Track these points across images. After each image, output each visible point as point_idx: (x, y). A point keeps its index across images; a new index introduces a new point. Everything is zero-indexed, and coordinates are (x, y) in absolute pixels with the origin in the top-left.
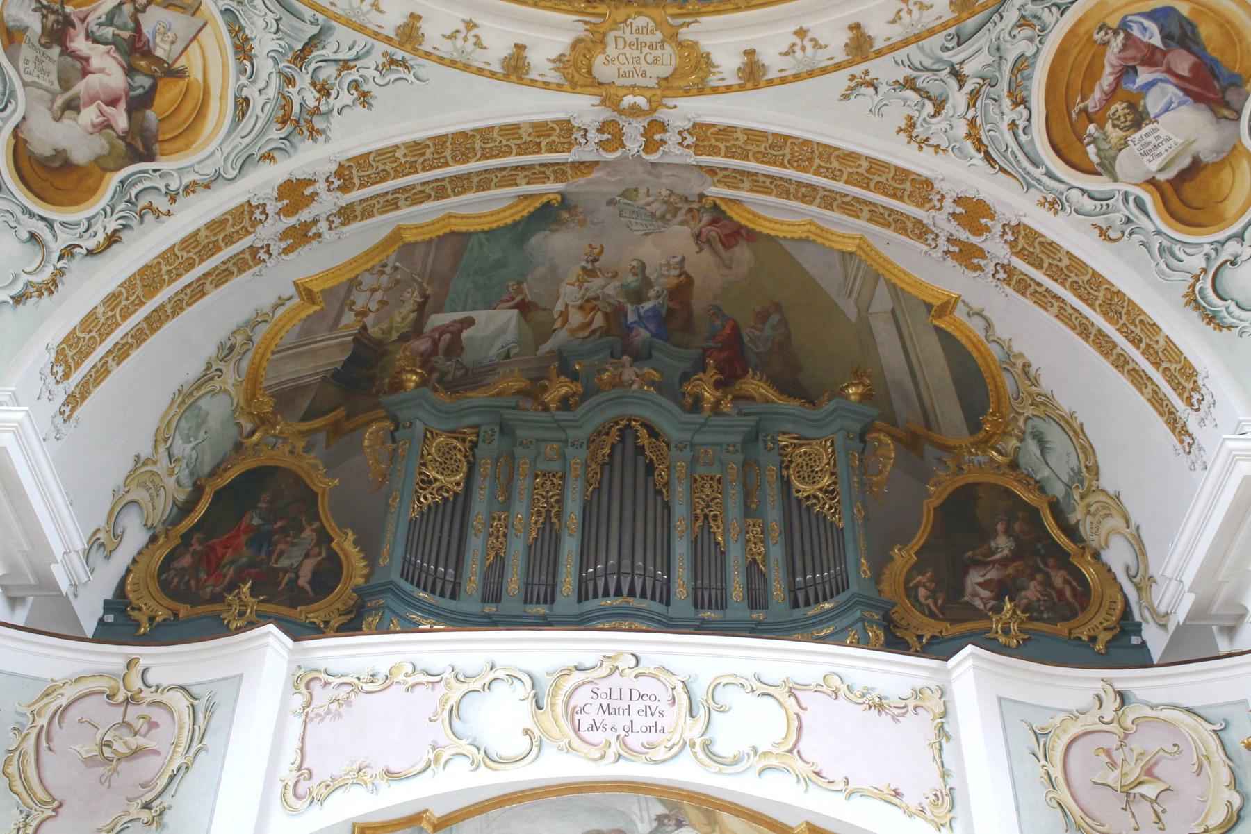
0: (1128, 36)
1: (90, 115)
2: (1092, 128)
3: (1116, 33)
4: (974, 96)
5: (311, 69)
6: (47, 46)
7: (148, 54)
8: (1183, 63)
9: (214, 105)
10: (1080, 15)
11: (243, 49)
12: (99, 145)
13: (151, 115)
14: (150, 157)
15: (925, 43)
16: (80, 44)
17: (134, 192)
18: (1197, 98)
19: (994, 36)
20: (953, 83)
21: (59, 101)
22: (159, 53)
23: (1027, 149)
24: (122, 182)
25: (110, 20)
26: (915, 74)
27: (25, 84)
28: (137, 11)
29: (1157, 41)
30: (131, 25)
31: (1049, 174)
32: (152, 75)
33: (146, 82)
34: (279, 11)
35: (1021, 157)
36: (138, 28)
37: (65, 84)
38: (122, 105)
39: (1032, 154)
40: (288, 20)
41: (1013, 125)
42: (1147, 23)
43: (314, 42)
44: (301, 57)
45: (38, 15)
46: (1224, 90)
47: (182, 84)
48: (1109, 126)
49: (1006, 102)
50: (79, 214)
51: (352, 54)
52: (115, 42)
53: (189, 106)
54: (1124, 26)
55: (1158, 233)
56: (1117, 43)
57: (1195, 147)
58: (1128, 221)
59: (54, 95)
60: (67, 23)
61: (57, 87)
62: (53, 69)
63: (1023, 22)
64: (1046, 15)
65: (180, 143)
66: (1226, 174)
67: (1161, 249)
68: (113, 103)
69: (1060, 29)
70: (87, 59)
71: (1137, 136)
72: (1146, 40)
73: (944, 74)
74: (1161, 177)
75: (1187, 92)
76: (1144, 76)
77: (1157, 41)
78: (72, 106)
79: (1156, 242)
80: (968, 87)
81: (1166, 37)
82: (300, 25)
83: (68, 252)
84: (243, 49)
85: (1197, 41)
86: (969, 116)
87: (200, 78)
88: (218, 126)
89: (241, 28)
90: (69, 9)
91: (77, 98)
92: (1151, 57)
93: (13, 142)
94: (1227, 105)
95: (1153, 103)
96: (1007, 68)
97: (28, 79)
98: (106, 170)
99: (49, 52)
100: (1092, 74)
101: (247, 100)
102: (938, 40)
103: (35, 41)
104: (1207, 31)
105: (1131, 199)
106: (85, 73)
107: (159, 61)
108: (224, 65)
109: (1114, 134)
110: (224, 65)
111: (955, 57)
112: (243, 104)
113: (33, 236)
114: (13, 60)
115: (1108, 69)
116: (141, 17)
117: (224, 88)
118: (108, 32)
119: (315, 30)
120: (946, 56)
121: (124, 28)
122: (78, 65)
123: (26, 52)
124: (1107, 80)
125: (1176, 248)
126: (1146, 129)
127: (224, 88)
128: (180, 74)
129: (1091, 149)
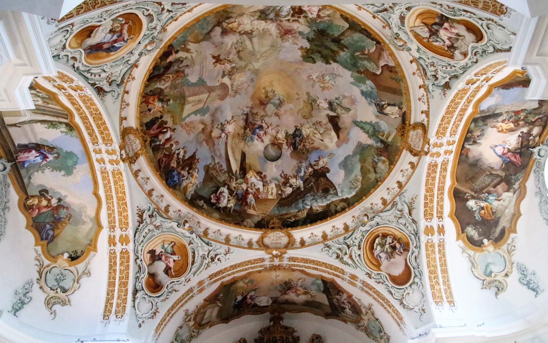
0: (123, 40)
1: (455, 31)
2: (124, 22)
3: (128, 39)
4: (163, 9)
5: (383, 7)
6: (457, 47)
7: (430, 31)
8: (105, 46)
9: (417, 13)
10: (139, 38)
11: (402, 19)
12: (455, 25)
13: (437, 20)
14: (442, 15)
15: (181, 13)
16: (448, 43)
17: (452, 13)
18: (98, 44)
19: (162, 23)
20: (170, 9)
21: (461, 38)
22: (427, 29)
23: (141, 9)
24: (454, 16)
25: (437, 41)
26: (184, 6)
27: (468, 46)
28: (429, 39)
29: (116, 45)
30: (432, 37)
31: (132, 9)
32: (431, 27)
33: (434, 26)
34: (388, 20)
35: (142, 7)
36: (430, 36)
37: (457, 40)
38: (443, 27)
39: (139, 9)
40: (387, 18)
41: (148, 10)
42: (121, 45)
43: (380, 12)
44: (386, 10)
45: (455, 53)
46: (92, 50)
47: (424, 21)
48: (119, 25)
49: (152, 13)
50: (471, 20)
51: (368, 6)
52: (438, 37)
53: (424, 17)
54: (126, 42)
55: (91, 22)
56: (126, 37)
57: (91, 38)
58: (101, 17)
59: (462, 40)
60: (448, 47)
61: (460, 41)
62: (458, 43)
63: (155, 28)
64: (149, 32)
65: (431, 12)
66: (79, 41)
67: (88, 21)
68: (446, 29)
69: (144, 31)
70: (448, 39)
71: (109, 29)
72: (119, 43)
73: (174, 10)
74: (97, 29)
75: (102, 43)
76: (115, 37)
77: (116, 45)
78: (457, 35)
79: (90, 20)
80: (165, 11)
81: (113, 47)
82: (383, 16)
83: (480, 19)
84: (402, 19)
85: (104, 51)
86: (162, 6)
87: (418, 20)
88: (417, 10)
89: (401, 22)
90: (447, 49)
91: (455, 35)
92: (115, 41)
93: (480, 42)
94: (89, 49)
95: (110, 36)
96: (155, 18)
97: (466, 46)
98: (458, 21)
99: (457, 46)
100: (130, 31)
101: (406, 9)
102: (178, 15)
103: (459, 50)
104: (104, 54)
105: (103, 20)
106: (450, 38)
107: (428, 28)
108: (409, 18)
109: (116, 25)
110: (409, 18)
111: (171, 14)
112: (408, 9)
113: (489, 28)
114: (467, 51)
115: (126, 33)
116: (428, 37)
117: (412, 15)
118: (438, 39)
119: (378, 13)
120: (175, 13)
121: (434, 38)
122: (451, 40)
123: (463, 50)
124: (125, 31)
125: (83, 24)
126: (108, 31)
127: (412, 15)
128: (423, 23)
129: (121, 19)
